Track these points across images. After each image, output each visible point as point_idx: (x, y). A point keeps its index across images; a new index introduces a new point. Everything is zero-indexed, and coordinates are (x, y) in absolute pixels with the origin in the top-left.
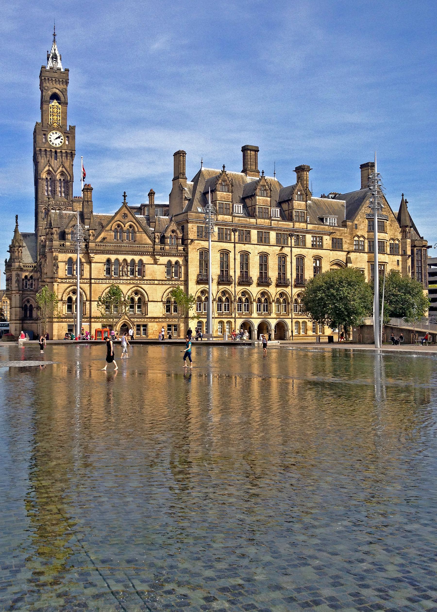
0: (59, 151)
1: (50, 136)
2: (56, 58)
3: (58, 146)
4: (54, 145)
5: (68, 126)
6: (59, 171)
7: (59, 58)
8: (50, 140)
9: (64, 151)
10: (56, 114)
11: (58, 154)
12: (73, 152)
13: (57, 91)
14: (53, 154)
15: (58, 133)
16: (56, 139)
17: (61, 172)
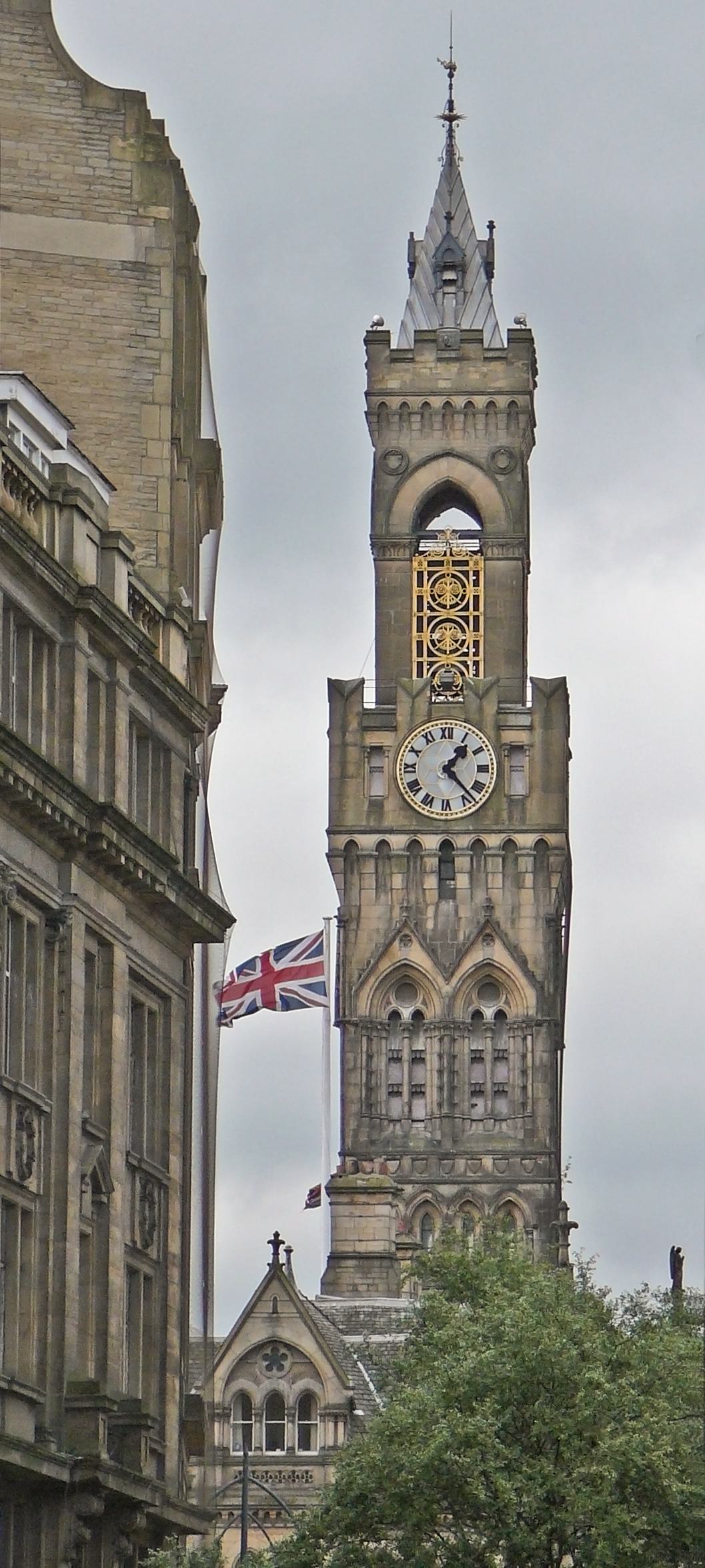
0: (463, 841)
1: (410, 758)
2: (461, 267)
3: (458, 810)
4: (437, 807)
5: (529, 684)
6: (468, 964)
7: (476, 261)
8: (410, 778)
9: (493, 841)
10: (453, 614)
11: (462, 862)
12: (553, 839)
13: (460, 472)
14: (431, 863)
15: (458, 733)
16: (448, 769)
17: (479, 967)
